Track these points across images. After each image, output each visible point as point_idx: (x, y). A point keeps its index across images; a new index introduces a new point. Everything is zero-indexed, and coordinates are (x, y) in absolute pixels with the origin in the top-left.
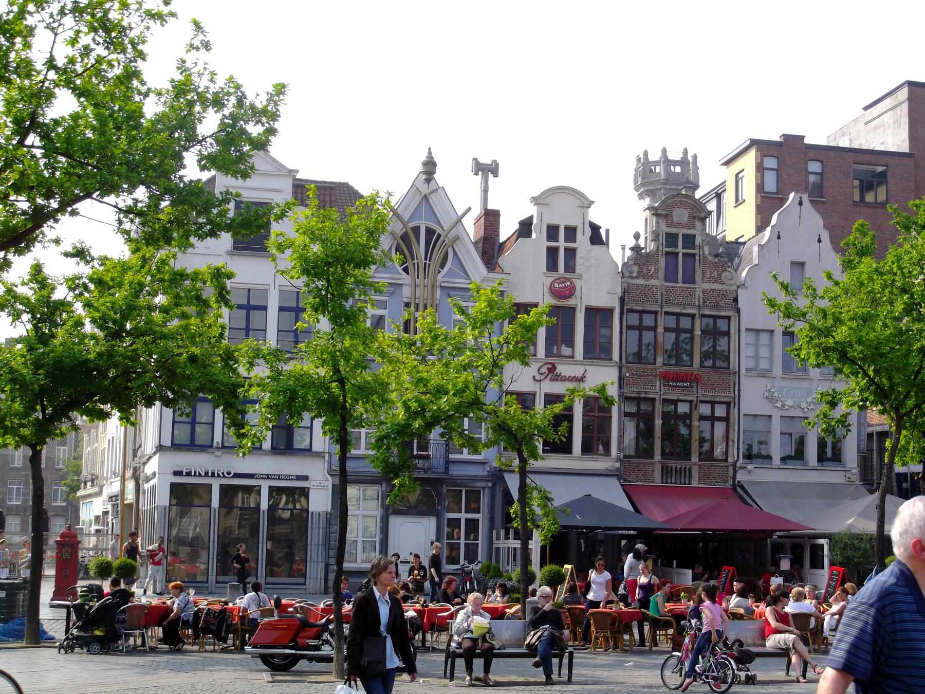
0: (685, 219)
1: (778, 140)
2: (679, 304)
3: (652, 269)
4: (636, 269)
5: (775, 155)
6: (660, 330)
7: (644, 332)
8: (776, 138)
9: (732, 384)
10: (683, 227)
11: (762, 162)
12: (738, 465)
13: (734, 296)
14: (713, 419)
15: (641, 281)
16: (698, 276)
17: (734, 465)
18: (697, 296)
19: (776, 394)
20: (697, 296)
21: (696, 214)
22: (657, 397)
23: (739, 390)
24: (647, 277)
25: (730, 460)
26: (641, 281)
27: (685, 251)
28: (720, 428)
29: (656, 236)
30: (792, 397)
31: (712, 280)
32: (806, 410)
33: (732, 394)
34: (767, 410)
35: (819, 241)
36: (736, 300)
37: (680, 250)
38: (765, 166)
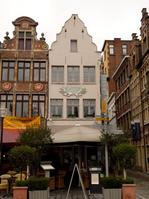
0: (27, 26)
1: (114, 40)
2: (23, 58)
3: (13, 45)
4: (6, 45)
5: (113, 44)
6: (16, 68)
7: (10, 69)
8: (113, 39)
9: (46, 87)
10: (26, 29)
11: (109, 46)
12: (47, 119)
13: (47, 54)
14: (39, 101)
15: (8, 50)
16: (32, 46)
17: (46, 120)
18: (31, 54)
19: (64, 90)
20: (31, 54)
21: (31, 24)
22: (14, 93)
23: (48, 89)
24: (11, 48)
25: (45, 118)
26: (8, 50)
27: (27, 38)
28: (42, 105)
29: (15, 33)
30: (71, 91)
31: (37, 48)
32: (77, 96)
33: (46, 91)
34: (60, 96)
35: (83, 32)
36: (48, 55)
37: (25, 38)
38: (110, 47)
